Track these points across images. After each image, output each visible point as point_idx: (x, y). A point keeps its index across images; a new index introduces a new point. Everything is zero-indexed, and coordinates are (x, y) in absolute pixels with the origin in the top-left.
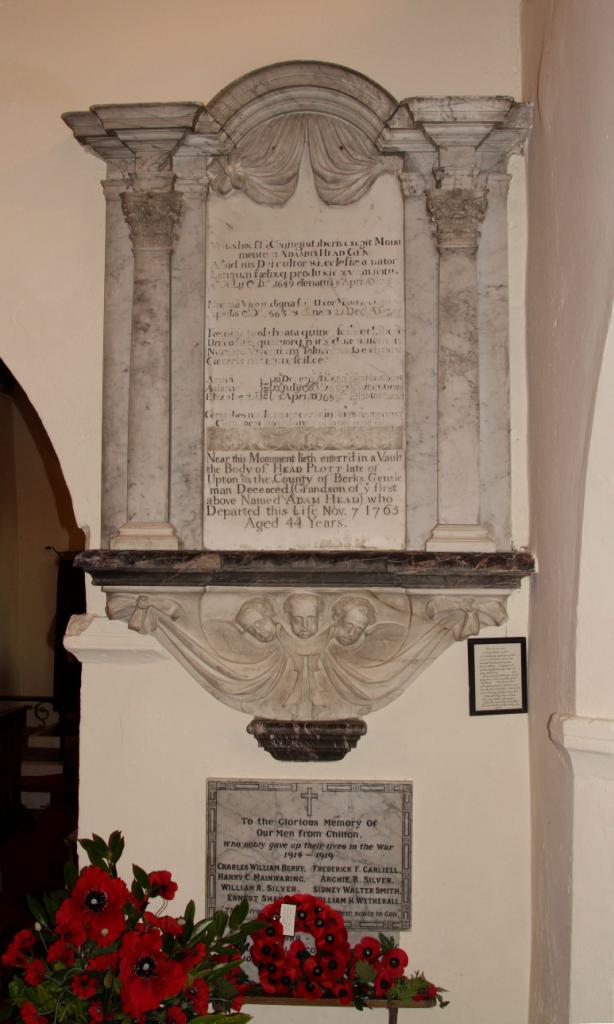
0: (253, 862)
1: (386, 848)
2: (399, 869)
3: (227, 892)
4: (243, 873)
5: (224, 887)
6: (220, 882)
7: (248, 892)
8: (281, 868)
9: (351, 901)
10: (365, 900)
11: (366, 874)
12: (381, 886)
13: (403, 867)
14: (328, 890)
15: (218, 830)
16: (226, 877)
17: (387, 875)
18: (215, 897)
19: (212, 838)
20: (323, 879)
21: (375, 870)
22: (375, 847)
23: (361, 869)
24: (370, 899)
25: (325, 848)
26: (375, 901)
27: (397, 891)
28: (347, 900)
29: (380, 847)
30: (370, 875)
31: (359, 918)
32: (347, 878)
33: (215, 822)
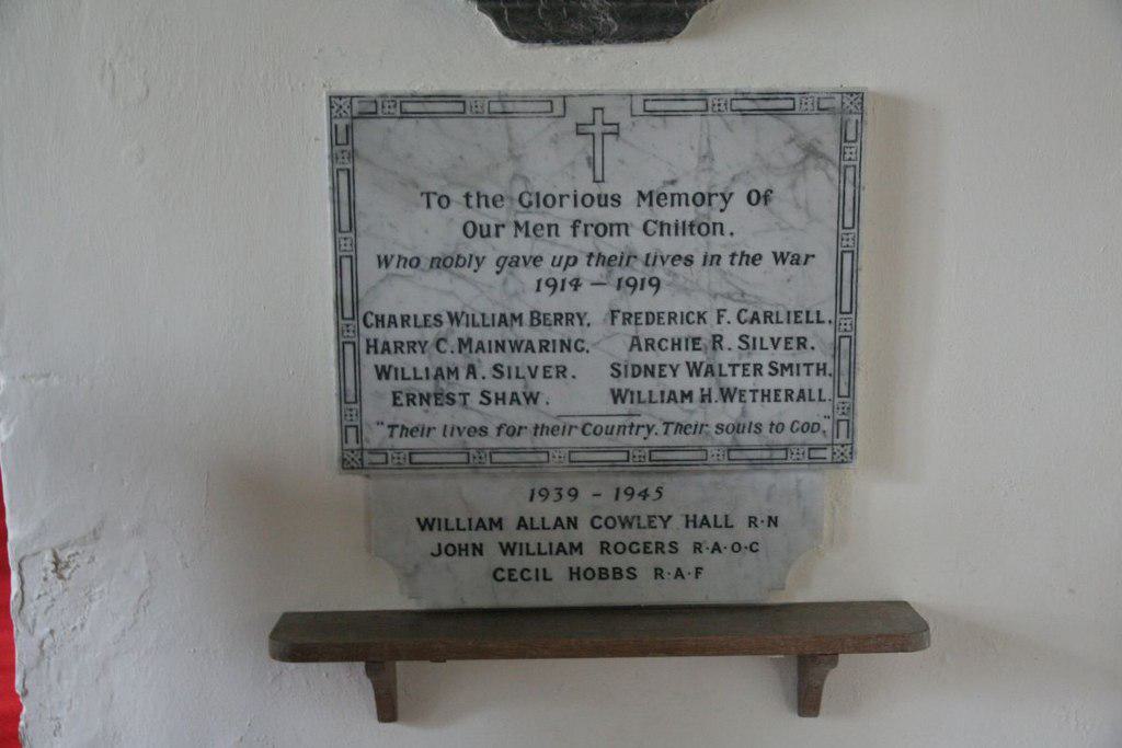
0: (456, 307)
1: (796, 261)
2: (828, 314)
3: (389, 386)
4: (430, 334)
5: (383, 373)
6: (370, 361)
7: (443, 384)
8: (526, 318)
9: (706, 397)
10: (742, 394)
11: (748, 329)
12: (782, 356)
13: (839, 310)
14: (649, 371)
15: (361, 224)
16: (386, 349)
17: (798, 331)
18: (358, 399)
19: (346, 246)
20: (635, 343)
21: (768, 316)
22: (768, 259)
23: (730, 316)
24: (754, 391)
25: (639, 265)
26: (765, 395)
27: (821, 369)
28: (697, 395)
29: (780, 258)
30: (754, 330)
31: (726, 439)
32: (696, 340)
33: (352, 205)
